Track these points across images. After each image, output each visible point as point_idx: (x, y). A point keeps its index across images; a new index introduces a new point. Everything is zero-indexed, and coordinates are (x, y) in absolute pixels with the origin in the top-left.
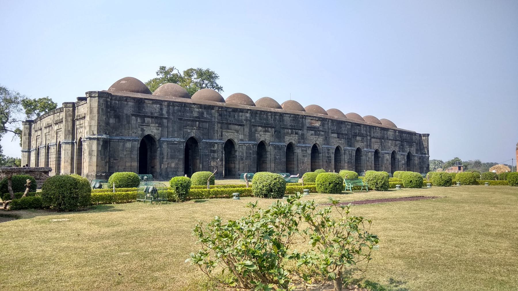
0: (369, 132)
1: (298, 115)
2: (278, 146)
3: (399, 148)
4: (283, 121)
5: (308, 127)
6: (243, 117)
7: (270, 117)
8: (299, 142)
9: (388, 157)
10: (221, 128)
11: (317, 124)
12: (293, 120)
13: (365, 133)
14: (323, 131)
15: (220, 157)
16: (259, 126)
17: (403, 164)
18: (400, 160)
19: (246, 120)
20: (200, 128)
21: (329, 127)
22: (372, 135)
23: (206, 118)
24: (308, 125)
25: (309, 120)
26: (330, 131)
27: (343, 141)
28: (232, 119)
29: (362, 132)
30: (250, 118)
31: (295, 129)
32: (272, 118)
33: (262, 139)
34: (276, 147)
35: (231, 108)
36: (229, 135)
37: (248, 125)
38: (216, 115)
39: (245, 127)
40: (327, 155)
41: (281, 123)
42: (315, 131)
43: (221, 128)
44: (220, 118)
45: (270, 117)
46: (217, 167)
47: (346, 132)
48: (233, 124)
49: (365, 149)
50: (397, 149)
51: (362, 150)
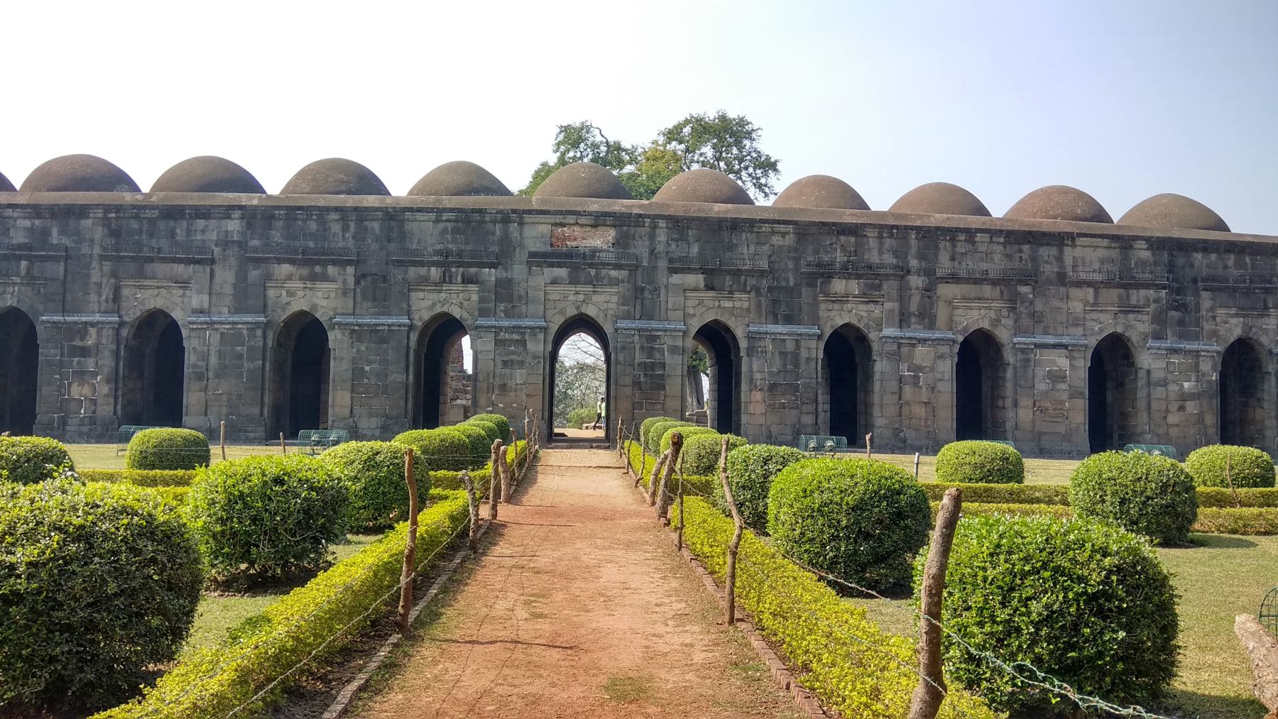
0: (922, 257)
1: (474, 211)
2: (374, 330)
4: (403, 236)
5: (532, 255)
6: (208, 233)
7: (336, 228)
8: (484, 313)
10: (114, 274)
11: (600, 240)
12: (456, 231)
13: (889, 259)
14: (618, 267)
15: (106, 370)
16: (280, 261)
17: (1184, 397)
18: (1157, 375)
19: (225, 243)
20: (33, 278)
21: (660, 248)
22: (944, 263)
23: (57, 247)
24: (534, 246)
25: (545, 229)
26: (662, 264)
27: (743, 301)
28: (164, 243)
29: (874, 257)
30: (243, 234)
31: (459, 265)
32: (345, 229)
33: (299, 304)
34: (357, 334)
35: (152, 207)
36: (143, 298)
37: (233, 261)
38: (99, 233)
39: (217, 269)
40: (639, 357)
41: (392, 246)
42: (574, 269)
43: (114, 274)
44: (111, 242)
45: (336, 228)
46: (94, 402)
47: (764, 264)
48: (164, 260)
49: (889, 331)
50: (1138, 328)
51: (873, 336)
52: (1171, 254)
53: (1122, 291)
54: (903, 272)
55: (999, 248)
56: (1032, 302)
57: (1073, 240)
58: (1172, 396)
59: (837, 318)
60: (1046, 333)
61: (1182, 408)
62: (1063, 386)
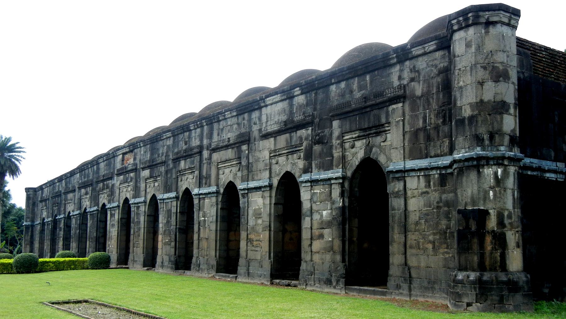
3: (308, 156)
8: (109, 202)
9: (260, 201)
17: (324, 225)
52: (316, 94)
53: (288, 135)
55: (234, 120)
57: (264, 102)
58: (315, 226)
60: (253, 180)
62: (260, 221)
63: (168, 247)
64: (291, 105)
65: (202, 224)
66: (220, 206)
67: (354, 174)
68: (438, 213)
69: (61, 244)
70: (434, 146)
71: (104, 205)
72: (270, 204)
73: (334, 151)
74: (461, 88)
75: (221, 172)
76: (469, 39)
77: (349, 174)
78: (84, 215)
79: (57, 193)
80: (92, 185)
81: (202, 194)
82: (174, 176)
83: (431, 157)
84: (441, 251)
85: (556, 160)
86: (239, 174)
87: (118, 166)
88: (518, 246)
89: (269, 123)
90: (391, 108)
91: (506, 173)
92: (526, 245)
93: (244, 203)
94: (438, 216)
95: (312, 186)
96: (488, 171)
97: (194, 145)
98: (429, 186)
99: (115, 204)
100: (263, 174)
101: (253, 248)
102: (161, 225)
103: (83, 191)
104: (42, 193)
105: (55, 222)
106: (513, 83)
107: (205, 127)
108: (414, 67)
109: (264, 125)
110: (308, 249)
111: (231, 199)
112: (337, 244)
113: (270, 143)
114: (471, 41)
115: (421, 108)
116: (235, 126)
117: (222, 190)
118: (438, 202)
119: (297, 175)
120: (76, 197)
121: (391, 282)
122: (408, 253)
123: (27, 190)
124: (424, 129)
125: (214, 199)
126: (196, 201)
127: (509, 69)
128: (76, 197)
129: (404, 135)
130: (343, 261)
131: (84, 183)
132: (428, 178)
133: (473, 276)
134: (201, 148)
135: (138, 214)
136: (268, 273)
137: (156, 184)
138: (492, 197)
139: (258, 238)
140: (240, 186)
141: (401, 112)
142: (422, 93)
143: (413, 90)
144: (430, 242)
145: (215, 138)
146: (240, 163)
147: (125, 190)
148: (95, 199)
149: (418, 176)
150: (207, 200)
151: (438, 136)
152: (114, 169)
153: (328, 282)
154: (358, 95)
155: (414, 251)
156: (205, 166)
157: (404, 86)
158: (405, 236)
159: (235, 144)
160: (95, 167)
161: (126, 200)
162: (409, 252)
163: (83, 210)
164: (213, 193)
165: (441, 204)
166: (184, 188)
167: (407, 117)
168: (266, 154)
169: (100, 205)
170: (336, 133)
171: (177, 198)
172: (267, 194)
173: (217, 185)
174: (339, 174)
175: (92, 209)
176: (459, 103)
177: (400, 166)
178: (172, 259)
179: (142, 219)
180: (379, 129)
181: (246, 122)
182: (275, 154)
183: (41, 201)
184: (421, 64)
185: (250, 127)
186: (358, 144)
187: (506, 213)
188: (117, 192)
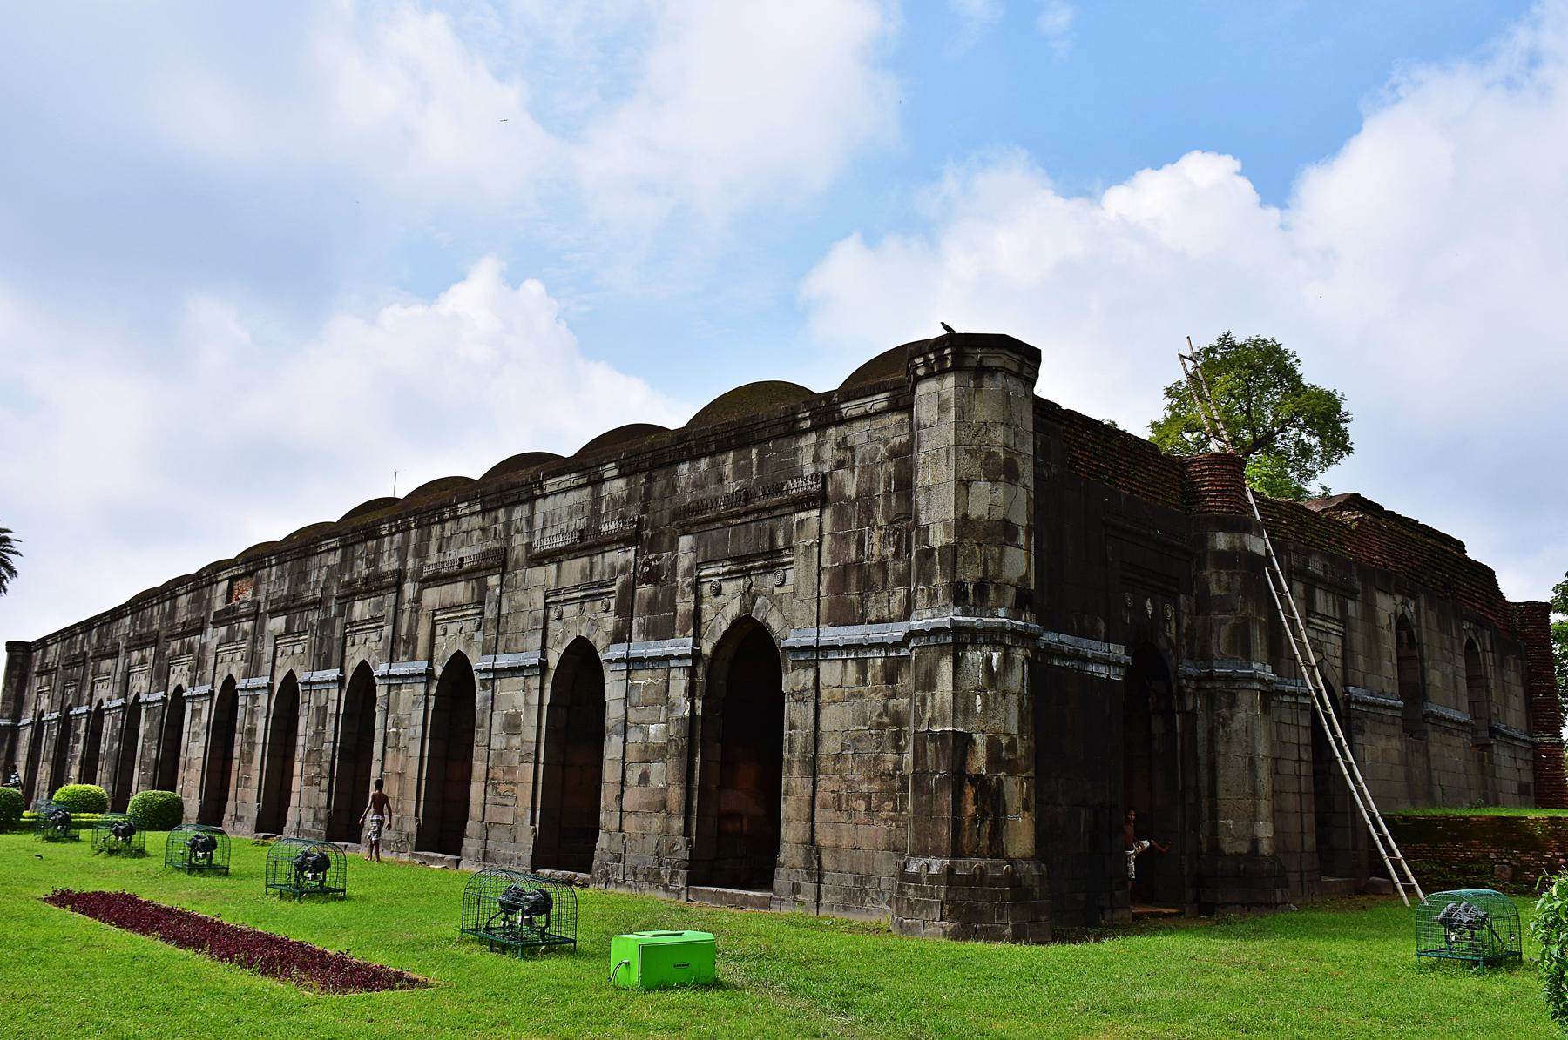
3: (625, 608)
9: (520, 697)
17: (650, 754)
50: (599, 624)
52: (650, 479)
53: (586, 560)
54: (400, 576)
55: (477, 521)
56: (499, 602)
57: (541, 487)
59: (355, 656)
61: (644, 779)
62: (516, 741)
63: (315, 789)
64: (596, 499)
65: (391, 741)
66: (432, 705)
67: (717, 648)
68: (881, 736)
69: (75, 771)
70: (877, 601)
71: (179, 689)
72: (541, 705)
73: (678, 600)
74: (928, 488)
75: (439, 631)
76: (945, 396)
77: (707, 648)
78: (132, 711)
79: (76, 656)
80: (156, 643)
81: (395, 676)
82: (338, 634)
83: (870, 622)
84: (884, 815)
85: (1108, 640)
86: (479, 637)
87: (219, 605)
88: (1026, 808)
89: (548, 533)
90: (796, 518)
91: (1007, 661)
92: (1040, 804)
93: (486, 700)
94: (879, 743)
95: (629, 672)
96: (974, 657)
97: (385, 568)
98: (865, 680)
99: (205, 689)
100: (530, 640)
101: (499, 800)
102: (300, 740)
103: (136, 655)
104: (44, 656)
105: (67, 722)
106: (1025, 486)
107: (414, 532)
108: (845, 439)
109: (538, 536)
110: (615, 806)
111: (455, 691)
112: (675, 795)
113: (544, 575)
114: (948, 400)
115: (854, 524)
116: (477, 534)
117: (439, 671)
118: (880, 715)
119: (599, 647)
120: (120, 669)
121: (782, 880)
122: (816, 819)
123: (12, 646)
124: (859, 564)
125: (421, 689)
126: (381, 692)
127: (1018, 460)
128: (120, 669)
129: (819, 575)
130: (686, 832)
131: (141, 637)
132: (862, 665)
133: (936, 865)
134: (400, 576)
135: (252, 712)
136: (527, 855)
137: (298, 649)
138: (979, 709)
139: (509, 778)
140: (478, 662)
141: (815, 526)
142: (858, 493)
143: (840, 487)
144: (861, 796)
145: (433, 557)
146: (482, 613)
147: (228, 658)
148: (160, 675)
149: (845, 660)
150: (405, 691)
151: (885, 581)
152: (208, 609)
153: (653, 878)
154: (731, 487)
155: (830, 814)
156: (407, 614)
157: (824, 477)
158: (814, 784)
159: (472, 571)
160: (167, 604)
161: (230, 681)
162: (820, 815)
163: (131, 698)
164: (420, 675)
165: (885, 720)
166: (357, 661)
167: (827, 539)
168: (538, 598)
169: (171, 690)
170: (685, 562)
171: (340, 681)
172: (535, 683)
173: (430, 659)
174: (687, 649)
175: (152, 698)
176: (923, 521)
177: (809, 638)
178: (322, 816)
179: (260, 724)
180: (771, 559)
181: (500, 527)
182: (556, 597)
183: (40, 674)
184: (858, 434)
185: (508, 537)
186: (728, 587)
187: (1004, 741)
188: (211, 661)
